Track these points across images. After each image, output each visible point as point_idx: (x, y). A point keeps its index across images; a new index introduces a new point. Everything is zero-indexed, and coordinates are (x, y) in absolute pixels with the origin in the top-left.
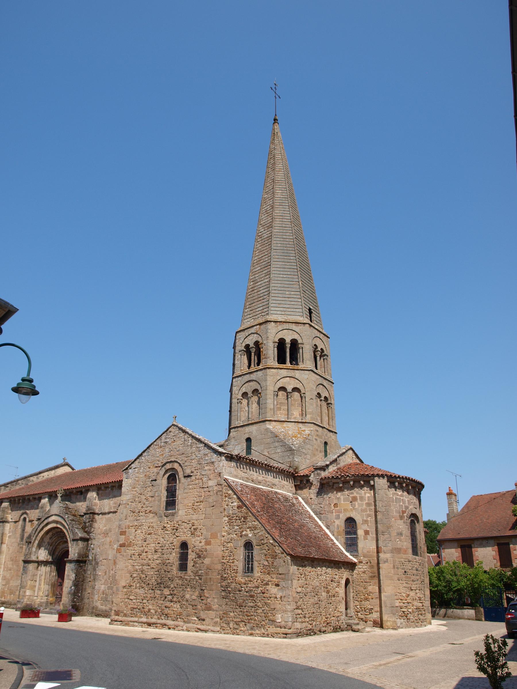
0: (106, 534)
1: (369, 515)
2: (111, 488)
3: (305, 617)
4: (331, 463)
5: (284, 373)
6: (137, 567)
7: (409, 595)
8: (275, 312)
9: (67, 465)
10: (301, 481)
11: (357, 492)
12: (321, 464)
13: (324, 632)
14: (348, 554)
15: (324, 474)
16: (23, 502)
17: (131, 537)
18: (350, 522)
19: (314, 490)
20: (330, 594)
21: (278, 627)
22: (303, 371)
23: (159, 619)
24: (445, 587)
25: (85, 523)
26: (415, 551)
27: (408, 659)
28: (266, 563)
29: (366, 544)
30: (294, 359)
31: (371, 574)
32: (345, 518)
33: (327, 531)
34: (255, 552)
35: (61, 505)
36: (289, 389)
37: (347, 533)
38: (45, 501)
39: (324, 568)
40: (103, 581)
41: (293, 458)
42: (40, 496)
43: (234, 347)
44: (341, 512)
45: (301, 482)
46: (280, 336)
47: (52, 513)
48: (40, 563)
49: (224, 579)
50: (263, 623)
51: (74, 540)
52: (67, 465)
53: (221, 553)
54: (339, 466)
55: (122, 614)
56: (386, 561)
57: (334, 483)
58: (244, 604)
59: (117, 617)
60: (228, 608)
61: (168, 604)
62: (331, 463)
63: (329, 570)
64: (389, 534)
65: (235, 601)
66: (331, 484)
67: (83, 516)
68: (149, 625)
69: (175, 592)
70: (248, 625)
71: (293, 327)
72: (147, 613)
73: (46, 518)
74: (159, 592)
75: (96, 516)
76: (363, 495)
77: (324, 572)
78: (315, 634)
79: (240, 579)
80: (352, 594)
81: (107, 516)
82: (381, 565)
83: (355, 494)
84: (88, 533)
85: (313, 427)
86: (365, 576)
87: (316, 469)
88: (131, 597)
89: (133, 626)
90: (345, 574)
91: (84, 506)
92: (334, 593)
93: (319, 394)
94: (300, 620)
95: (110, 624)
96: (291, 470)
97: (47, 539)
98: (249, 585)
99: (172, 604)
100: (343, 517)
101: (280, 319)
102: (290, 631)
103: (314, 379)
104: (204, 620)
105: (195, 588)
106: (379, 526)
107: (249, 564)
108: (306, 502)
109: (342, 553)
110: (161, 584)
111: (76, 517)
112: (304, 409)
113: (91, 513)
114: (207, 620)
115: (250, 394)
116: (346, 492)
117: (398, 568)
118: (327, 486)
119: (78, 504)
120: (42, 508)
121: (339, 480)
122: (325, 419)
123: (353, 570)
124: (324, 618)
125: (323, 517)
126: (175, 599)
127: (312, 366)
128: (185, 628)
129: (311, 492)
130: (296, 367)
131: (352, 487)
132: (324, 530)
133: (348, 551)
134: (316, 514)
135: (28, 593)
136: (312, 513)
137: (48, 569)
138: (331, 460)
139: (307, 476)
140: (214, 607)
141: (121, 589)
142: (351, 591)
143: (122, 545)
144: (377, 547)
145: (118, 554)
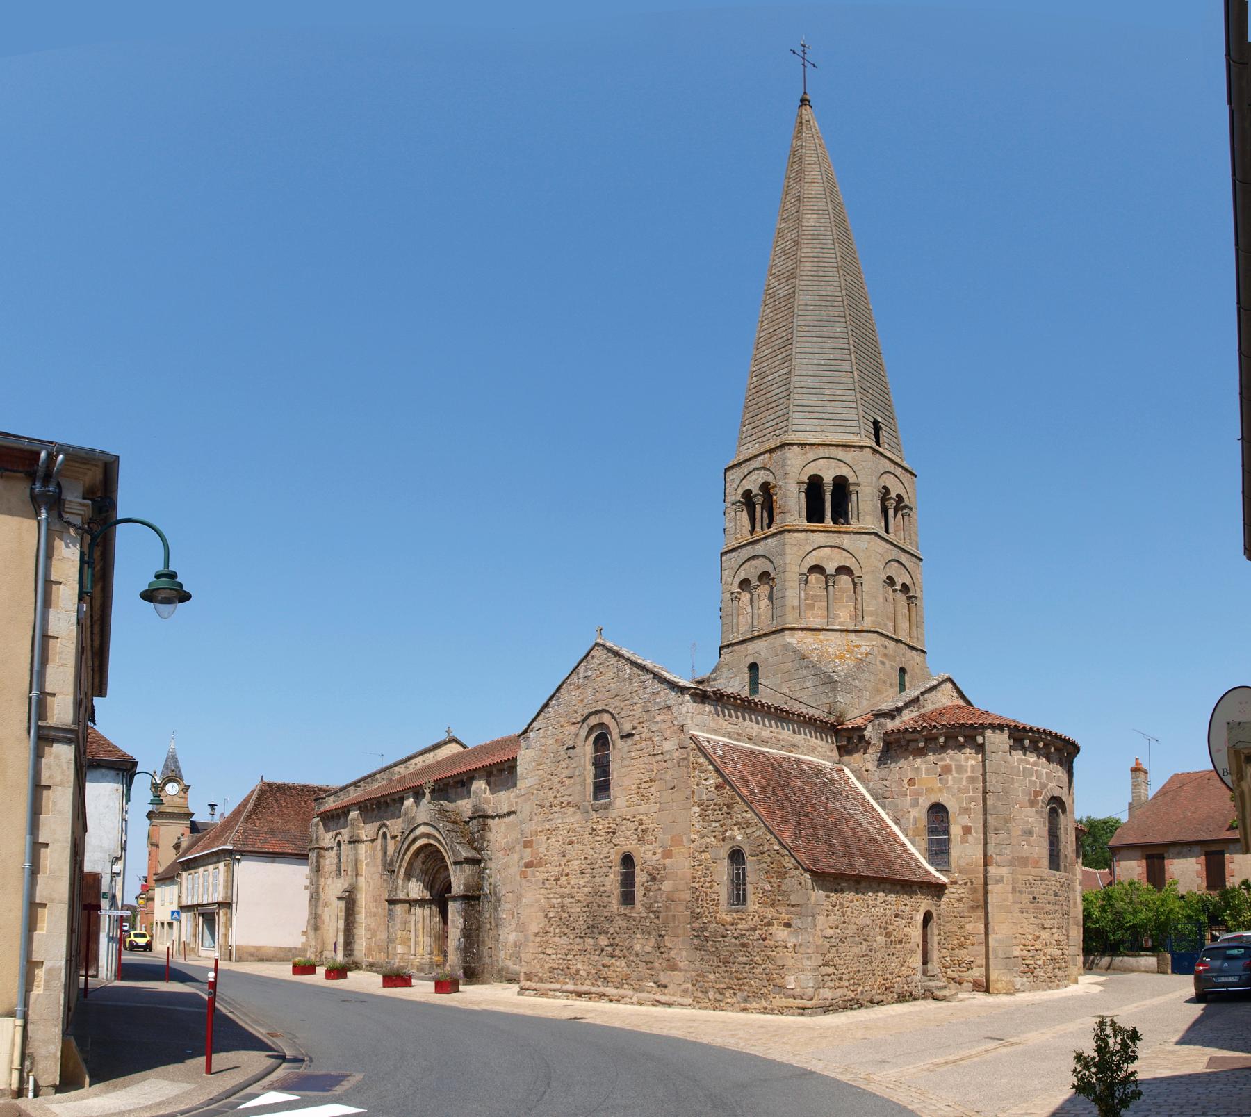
0: (509, 849)
1: (972, 800)
2: (501, 772)
3: (841, 979)
4: (907, 705)
5: (820, 539)
6: (554, 901)
7: (1038, 937)
8: (802, 428)
9: (454, 740)
10: (849, 739)
11: (951, 758)
12: (884, 706)
13: (880, 1003)
14: (931, 869)
15: (890, 725)
16: (379, 807)
17: (541, 850)
18: (938, 810)
19: (873, 754)
20: (893, 938)
21: (789, 997)
22: (858, 536)
23: (593, 985)
24: (1113, 921)
25: (472, 834)
26: (1055, 860)
27: (1004, 1050)
28: (768, 887)
29: (965, 851)
31: (971, 904)
32: (927, 805)
33: (896, 829)
34: (748, 867)
35: (432, 807)
36: (830, 569)
37: (932, 831)
38: (409, 802)
39: (881, 894)
40: (514, 926)
41: (835, 697)
42: (400, 795)
44: (921, 794)
45: (849, 740)
46: (812, 470)
47: (419, 821)
48: (412, 903)
49: (696, 916)
50: (765, 990)
51: (456, 863)
52: (454, 740)
53: (688, 872)
54: (923, 711)
55: (536, 979)
56: (1000, 880)
57: (909, 741)
58: (731, 960)
59: (528, 984)
60: (705, 966)
61: (607, 961)
62: (907, 705)
63: (891, 898)
64: (1008, 832)
65: (716, 953)
66: (903, 742)
67: (467, 823)
68: (579, 995)
69: (617, 941)
70: (739, 994)
71: (840, 453)
72: (575, 976)
73: (412, 831)
74: (591, 941)
75: (490, 821)
76: (963, 762)
77: (880, 900)
78: (861, 1006)
79: (724, 915)
80: (936, 938)
81: (506, 820)
82: (990, 887)
83: (948, 761)
84: (479, 850)
85: (876, 640)
86: (962, 907)
87: (877, 716)
88: (549, 951)
89: (555, 997)
90: (924, 903)
91: (469, 806)
92: (900, 936)
93: (889, 578)
94: (832, 984)
95: (519, 994)
96: (832, 719)
97: (418, 865)
98: (740, 926)
99: (613, 960)
100: (925, 803)
101: (811, 439)
102: (810, 1004)
103: (880, 550)
104: (665, 987)
105: (649, 933)
106: (989, 817)
107: (738, 890)
108: (857, 777)
109: (921, 867)
110: (593, 929)
111: (458, 825)
112: (859, 606)
113: (482, 817)
114: (671, 986)
116: (932, 757)
117: (1020, 892)
118: (897, 746)
119: (459, 802)
120: (406, 814)
121: (918, 736)
123: (939, 898)
124: (880, 979)
125: (885, 803)
126: (617, 953)
127: (875, 524)
128: (635, 1000)
129: (868, 760)
130: (844, 528)
131: (943, 748)
132: (888, 827)
133: (931, 863)
134: (876, 799)
135: (400, 950)
136: (869, 797)
137: (427, 911)
138: (907, 700)
139: (860, 729)
140: (681, 965)
141: (532, 938)
142: (936, 932)
143: (529, 865)
144: (985, 856)
145: (524, 881)
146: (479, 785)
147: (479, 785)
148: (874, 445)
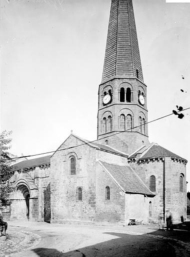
18: (153, 177)
30: (129, 100)
43: (99, 94)
115: (107, 118)
122: (143, 131)
146: (37, 168)
147: (37, 168)
148: (136, 78)
